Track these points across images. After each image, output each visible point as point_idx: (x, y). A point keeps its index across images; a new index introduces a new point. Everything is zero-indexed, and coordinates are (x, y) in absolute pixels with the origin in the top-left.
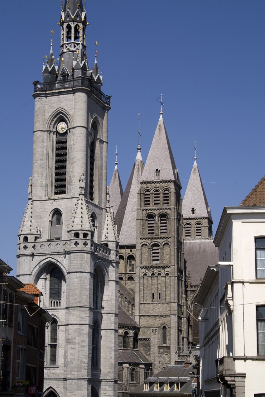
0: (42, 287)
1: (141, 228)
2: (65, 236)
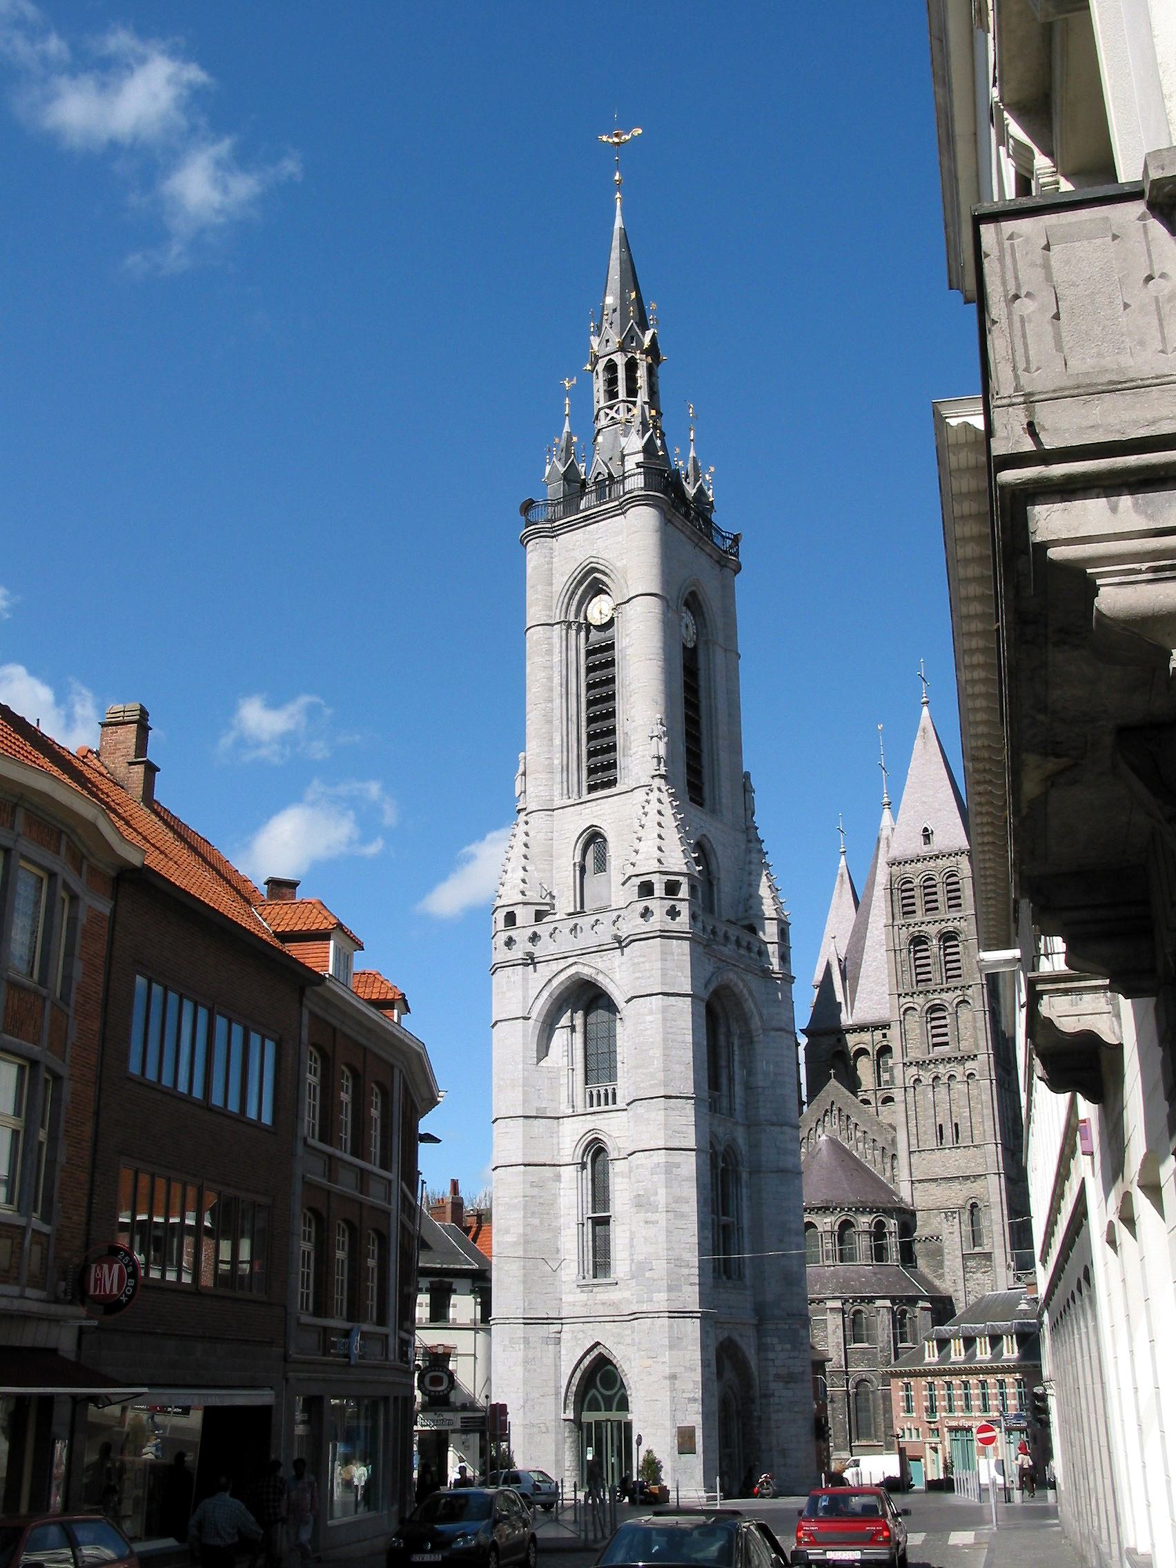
0: (564, 1051)
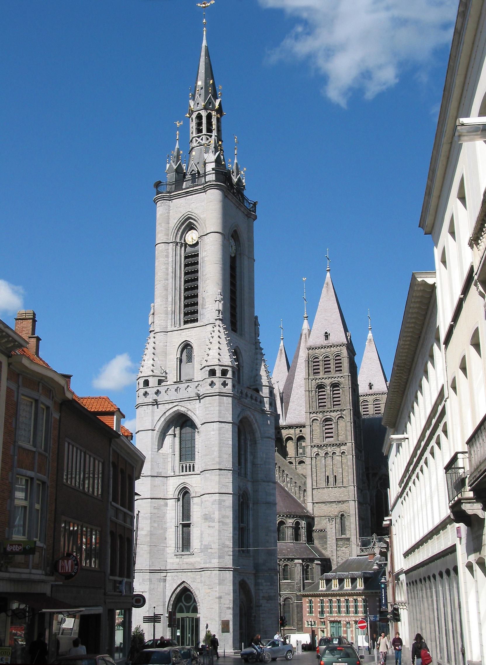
0: (170, 446)
1: (311, 401)
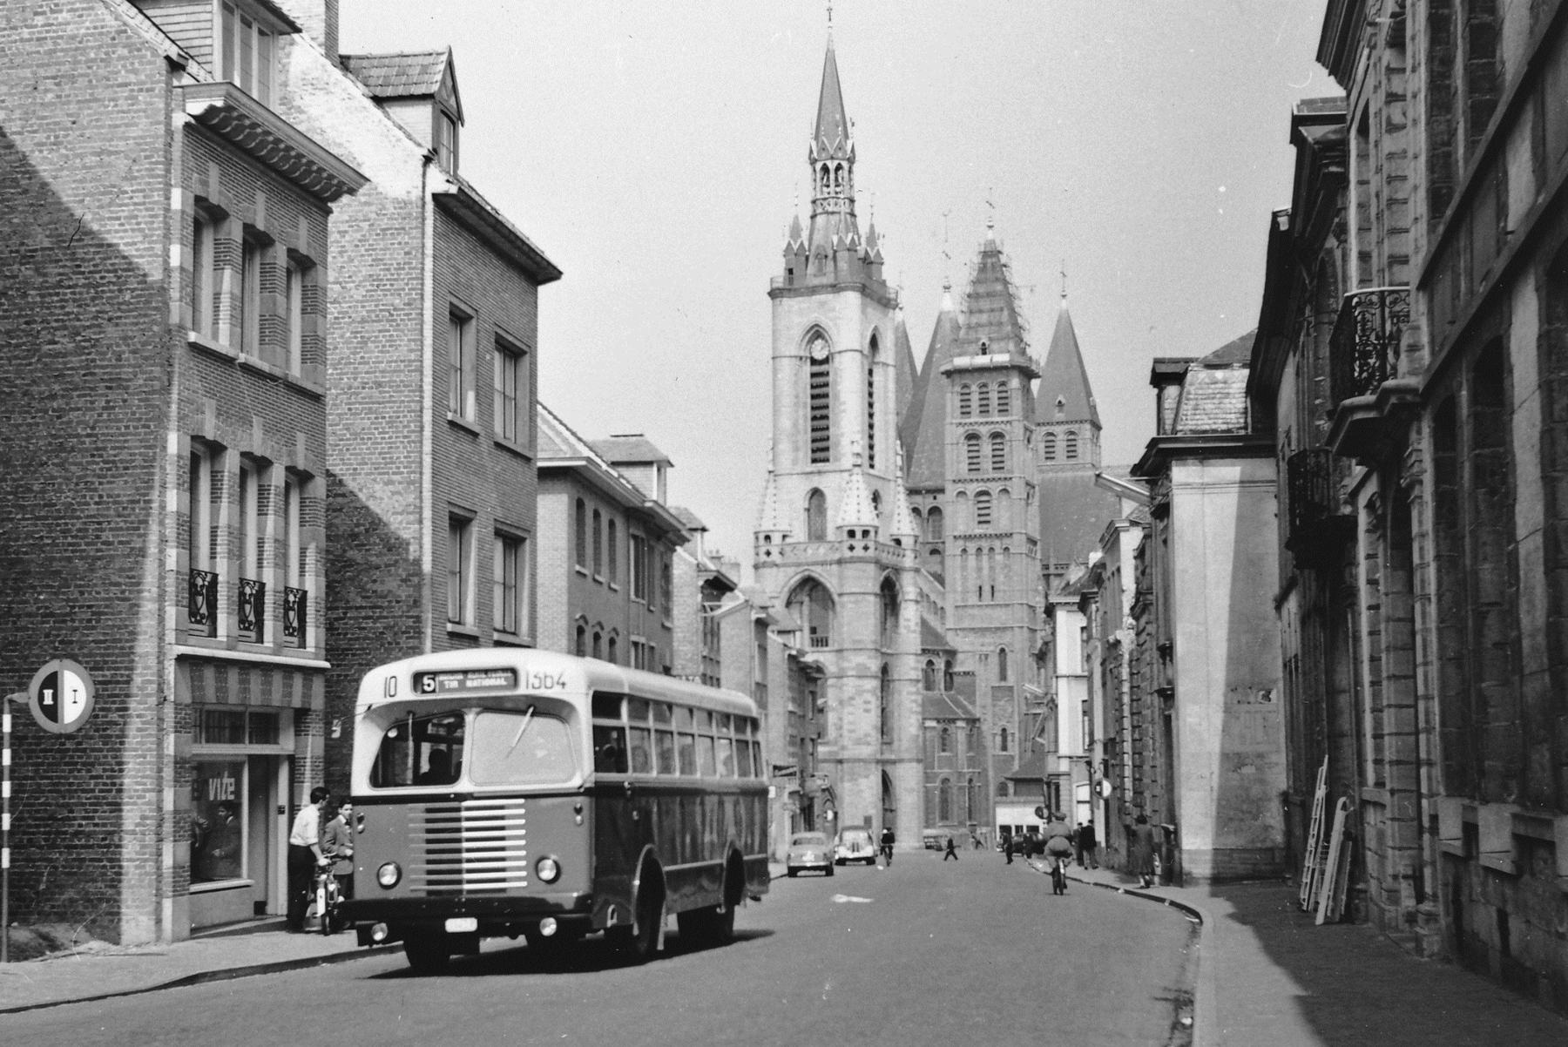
2: (831, 535)
